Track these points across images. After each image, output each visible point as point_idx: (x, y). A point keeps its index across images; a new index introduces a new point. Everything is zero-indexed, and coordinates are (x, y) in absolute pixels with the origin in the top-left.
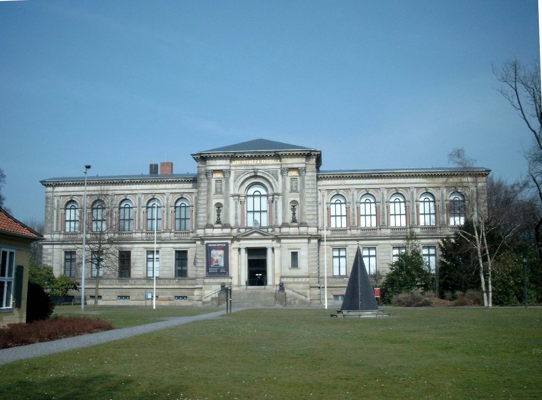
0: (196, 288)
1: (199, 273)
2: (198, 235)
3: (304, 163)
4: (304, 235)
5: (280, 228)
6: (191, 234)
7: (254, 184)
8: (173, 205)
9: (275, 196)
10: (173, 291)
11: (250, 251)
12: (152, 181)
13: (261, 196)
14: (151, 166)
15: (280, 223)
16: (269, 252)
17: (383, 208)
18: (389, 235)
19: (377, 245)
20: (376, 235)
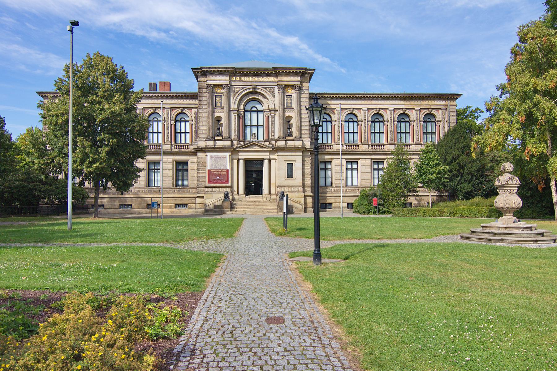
0: (198, 197)
1: (200, 183)
2: (199, 146)
3: (299, 81)
4: (299, 148)
5: (276, 141)
6: (191, 147)
7: (251, 100)
8: (174, 119)
9: (272, 112)
10: (174, 200)
11: (248, 162)
12: (152, 96)
13: (257, 111)
14: (150, 84)
15: (276, 137)
16: (266, 163)
17: (365, 126)
18: (370, 150)
19: (359, 159)
20: (358, 151)
